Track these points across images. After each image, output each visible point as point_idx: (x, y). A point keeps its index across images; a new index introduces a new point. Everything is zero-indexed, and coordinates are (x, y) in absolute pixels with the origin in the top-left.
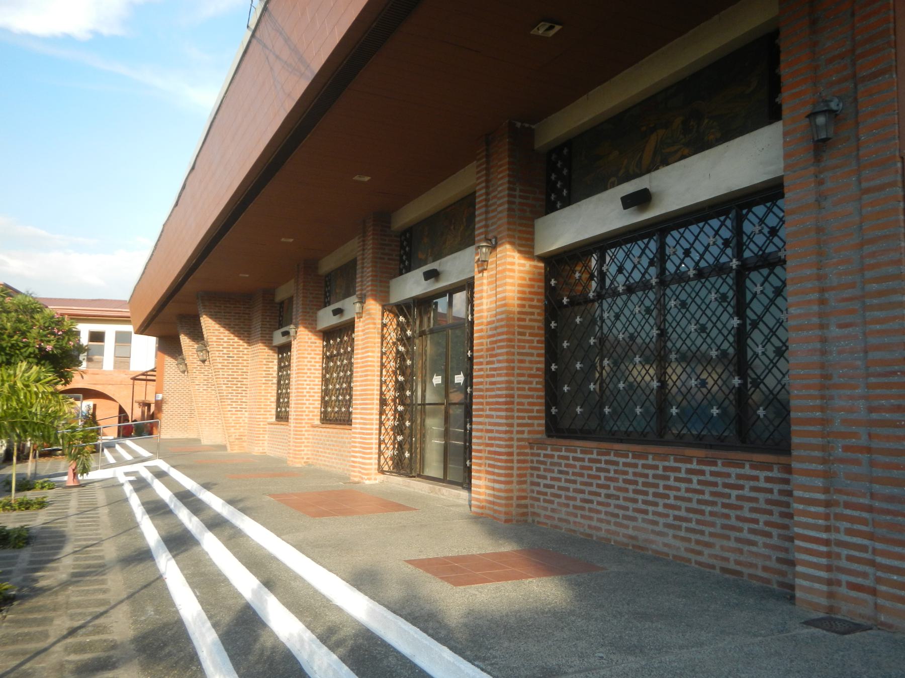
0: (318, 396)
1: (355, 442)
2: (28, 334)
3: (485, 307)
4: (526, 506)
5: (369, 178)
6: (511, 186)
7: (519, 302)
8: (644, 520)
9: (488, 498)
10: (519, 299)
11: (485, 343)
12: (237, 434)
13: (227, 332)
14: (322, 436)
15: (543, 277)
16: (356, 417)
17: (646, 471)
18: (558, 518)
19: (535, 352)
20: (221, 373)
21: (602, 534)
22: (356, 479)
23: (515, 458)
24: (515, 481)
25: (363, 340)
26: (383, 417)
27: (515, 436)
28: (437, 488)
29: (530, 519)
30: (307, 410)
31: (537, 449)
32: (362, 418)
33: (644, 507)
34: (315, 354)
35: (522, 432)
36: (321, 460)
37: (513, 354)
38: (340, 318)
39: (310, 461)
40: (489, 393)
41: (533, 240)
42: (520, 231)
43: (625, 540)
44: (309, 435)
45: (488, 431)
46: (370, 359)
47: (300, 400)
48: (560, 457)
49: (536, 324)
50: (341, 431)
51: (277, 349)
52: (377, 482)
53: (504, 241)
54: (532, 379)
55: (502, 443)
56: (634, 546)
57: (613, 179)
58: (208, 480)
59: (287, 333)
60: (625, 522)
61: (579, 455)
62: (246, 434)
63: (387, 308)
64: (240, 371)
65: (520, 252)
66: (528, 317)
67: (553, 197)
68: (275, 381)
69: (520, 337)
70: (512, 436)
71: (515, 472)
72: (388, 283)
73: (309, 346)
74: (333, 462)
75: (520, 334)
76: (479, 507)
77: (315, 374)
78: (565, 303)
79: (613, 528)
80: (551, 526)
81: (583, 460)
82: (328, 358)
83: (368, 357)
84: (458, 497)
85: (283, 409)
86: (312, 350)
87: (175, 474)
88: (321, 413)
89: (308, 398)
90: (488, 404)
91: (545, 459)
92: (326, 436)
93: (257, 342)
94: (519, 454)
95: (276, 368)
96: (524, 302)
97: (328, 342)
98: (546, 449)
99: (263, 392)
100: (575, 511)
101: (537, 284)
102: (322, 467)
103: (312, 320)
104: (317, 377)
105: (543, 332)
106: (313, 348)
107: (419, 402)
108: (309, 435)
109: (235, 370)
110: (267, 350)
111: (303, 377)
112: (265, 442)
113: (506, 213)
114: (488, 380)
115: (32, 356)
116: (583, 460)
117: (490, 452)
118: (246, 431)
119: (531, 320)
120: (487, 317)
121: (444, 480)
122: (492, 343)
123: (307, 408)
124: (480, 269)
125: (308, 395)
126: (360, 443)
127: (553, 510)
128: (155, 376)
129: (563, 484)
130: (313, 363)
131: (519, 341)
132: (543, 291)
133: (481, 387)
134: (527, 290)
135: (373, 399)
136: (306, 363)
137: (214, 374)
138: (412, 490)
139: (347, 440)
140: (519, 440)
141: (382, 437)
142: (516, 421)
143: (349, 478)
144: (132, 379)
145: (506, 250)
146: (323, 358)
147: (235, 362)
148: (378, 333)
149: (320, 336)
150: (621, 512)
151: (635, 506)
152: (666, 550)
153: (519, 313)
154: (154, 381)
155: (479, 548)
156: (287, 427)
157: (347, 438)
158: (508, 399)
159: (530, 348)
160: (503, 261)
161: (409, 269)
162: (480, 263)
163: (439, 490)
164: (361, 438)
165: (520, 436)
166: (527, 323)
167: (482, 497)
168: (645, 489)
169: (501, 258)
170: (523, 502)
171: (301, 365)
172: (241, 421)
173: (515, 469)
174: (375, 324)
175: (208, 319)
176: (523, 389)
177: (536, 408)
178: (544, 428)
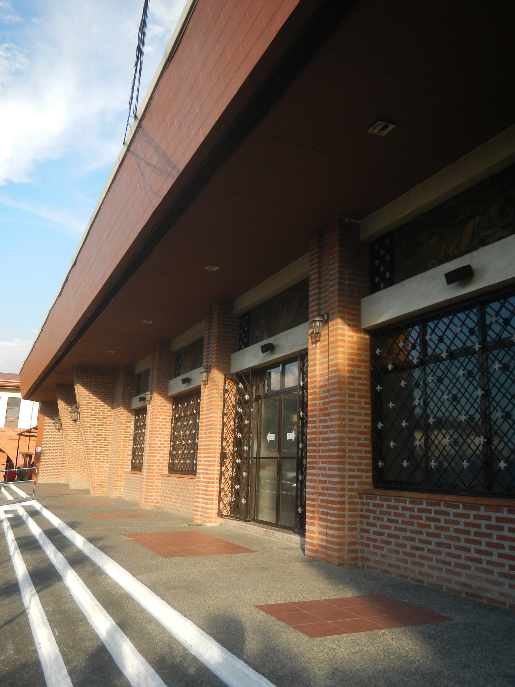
0: (167, 451)
1: (198, 489)
3: (318, 373)
4: (356, 551)
5: (218, 268)
6: (341, 270)
7: (349, 368)
8: (477, 569)
9: (321, 543)
10: (349, 365)
11: (318, 405)
12: (99, 481)
13: (95, 398)
14: (170, 483)
15: (368, 347)
16: (200, 469)
17: (478, 522)
18: (388, 564)
19: (363, 412)
20: (89, 431)
21: (434, 581)
22: (199, 522)
23: (347, 506)
24: (347, 528)
25: (207, 403)
26: (224, 468)
27: (347, 487)
28: (271, 531)
29: (360, 563)
30: (158, 462)
31: (366, 499)
32: (205, 469)
33: (477, 556)
34: (166, 416)
35: (352, 483)
36: (168, 504)
37: (344, 413)
38: (188, 385)
39: (159, 505)
40: (321, 448)
41: (359, 315)
42: (349, 308)
43: (459, 588)
44: (158, 482)
45: (321, 482)
46: (213, 419)
47: (152, 453)
48: (389, 507)
49: (364, 388)
50: (187, 480)
52: (217, 525)
53: (335, 316)
54: (360, 436)
55: (334, 492)
56: (467, 594)
57: (433, 261)
58: (73, 519)
59: (143, 399)
60: (458, 570)
61: (408, 505)
62: (106, 480)
63: (228, 376)
64: (104, 429)
65: (349, 325)
66: (356, 382)
67: (377, 279)
68: (132, 438)
69: (350, 399)
70: (344, 486)
71: (347, 520)
72: (230, 356)
73: (161, 409)
74: (178, 507)
75: (350, 396)
76: (312, 551)
77: (165, 431)
78: (390, 369)
79: (445, 575)
80: (381, 570)
81: (412, 510)
82: (176, 419)
83: (212, 417)
84: (291, 540)
85: (138, 461)
86: (163, 412)
87: (47, 513)
88: (169, 464)
89: (159, 451)
90: (321, 457)
91: (375, 508)
92: (173, 484)
93: (118, 406)
94: (350, 503)
96: (353, 369)
97: (177, 406)
98: (376, 499)
99: (122, 446)
100: (405, 558)
101: (363, 353)
102: (169, 510)
103: (164, 388)
104: (167, 435)
105: (369, 394)
106: (164, 411)
107: (255, 456)
108: (158, 482)
109: (100, 428)
110: (126, 412)
111: (156, 434)
112: (122, 488)
113: (337, 293)
114: (321, 436)
116: (412, 510)
117: (323, 501)
118: (106, 478)
119: (359, 384)
120: (320, 382)
121: (277, 525)
122: (324, 404)
123: (157, 460)
124: (314, 340)
125: (159, 449)
126: (202, 490)
127: (383, 556)
128: (36, 433)
129: (392, 532)
130: (164, 423)
131: (350, 402)
132: (368, 359)
133: (314, 442)
134: (356, 358)
135: (215, 453)
136: (158, 423)
137: (83, 431)
138: (248, 533)
139: (190, 488)
140: (350, 490)
141: (222, 486)
142: (348, 473)
143: (193, 521)
144: (18, 435)
145: (337, 323)
146: (172, 419)
148: (221, 397)
150: (453, 561)
151: (467, 554)
152: (502, 599)
153: (349, 377)
154: (35, 437)
155: (322, 593)
156: (140, 476)
157: (191, 486)
158: (340, 453)
159: (359, 408)
160: (335, 333)
161: (247, 345)
162: (313, 335)
163: (273, 533)
164: (204, 486)
165: (350, 487)
166: (356, 386)
167: (315, 542)
168: (477, 538)
169: (333, 331)
170: (353, 547)
171: (154, 424)
172: (103, 470)
173: (347, 516)
174: (218, 389)
175: (81, 387)
176: (353, 445)
177: (364, 462)
178: (371, 480)
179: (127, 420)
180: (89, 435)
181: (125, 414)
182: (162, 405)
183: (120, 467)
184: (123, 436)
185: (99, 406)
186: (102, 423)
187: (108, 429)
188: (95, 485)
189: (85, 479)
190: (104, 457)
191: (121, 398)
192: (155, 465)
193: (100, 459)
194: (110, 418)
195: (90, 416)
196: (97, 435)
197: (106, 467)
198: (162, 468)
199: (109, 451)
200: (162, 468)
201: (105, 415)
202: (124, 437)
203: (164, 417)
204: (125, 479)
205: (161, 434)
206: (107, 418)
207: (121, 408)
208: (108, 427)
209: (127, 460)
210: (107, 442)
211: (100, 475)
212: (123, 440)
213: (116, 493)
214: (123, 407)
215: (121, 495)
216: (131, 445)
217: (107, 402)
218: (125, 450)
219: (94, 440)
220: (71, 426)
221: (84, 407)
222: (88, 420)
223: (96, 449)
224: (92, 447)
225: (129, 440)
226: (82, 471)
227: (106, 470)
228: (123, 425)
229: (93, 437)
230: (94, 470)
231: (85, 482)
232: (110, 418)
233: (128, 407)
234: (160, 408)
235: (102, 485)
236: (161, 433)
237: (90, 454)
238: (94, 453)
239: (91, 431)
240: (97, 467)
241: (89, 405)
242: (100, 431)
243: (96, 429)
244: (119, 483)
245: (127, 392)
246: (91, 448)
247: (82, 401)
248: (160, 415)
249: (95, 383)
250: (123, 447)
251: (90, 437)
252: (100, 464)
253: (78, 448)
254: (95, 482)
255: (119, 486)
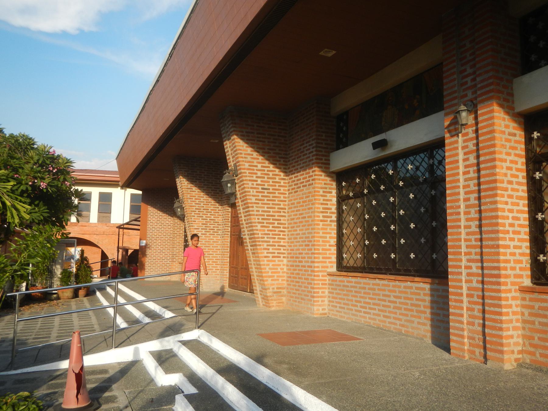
2: (20, 170)
12: (275, 287)
13: (261, 158)
20: (255, 209)
30: (512, 258)
39: (528, 359)
51: (334, 176)
62: (286, 286)
64: (276, 207)
68: (334, 217)
77: (517, 190)
89: (512, 236)
93: (307, 166)
95: (334, 200)
99: (321, 232)
103: (508, 94)
106: (512, 144)
109: (271, 206)
111: (503, 196)
115: (25, 195)
118: (285, 282)
125: (511, 229)
130: (514, 172)
136: (504, 171)
144: (117, 227)
147: (271, 195)
149: (519, 123)
172: (279, 270)
175: (239, 140)
179: (326, 188)
180: (257, 215)
181: (323, 180)
182: (507, 131)
183: (320, 265)
184: (321, 215)
185: (268, 171)
186: (273, 197)
187: (282, 206)
188: (269, 292)
189: (218, 278)
190: (280, 249)
191: (314, 153)
192: (508, 265)
193: (274, 253)
194: (284, 190)
195: (255, 186)
196: (267, 216)
197: (284, 265)
198: (521, 273)
199: (287, 240)
200: (521, 273)
201: (277, 184)
202: (324, 217)
203: (512, 158)
204: (329, 284)
205: (510, 197)
206: (280, 190)
207: (316, 169)
208: (282, 203)
209: (330, 254)
210: (282, 226)
211: (275, 278)
212: (321, 221)
213: (317, 307)
214: (319, 167)
215: (325, 312)
216: (333, 229)
217: (278, 165)
218: (326, 237)
219: (263, 223)
220: (197, 210)
221: (245, 173)
222: (253, 192)
223: (267, 238)
224: (262, 234)
225: (331, 221)
226: (214, 269)
227: (283, 269)
228: (321, 198)
229: (263, 219)
230: (267, 270)
231: (219, 282)
232: (284, 190)
233: (325, 168)
234: (504, 137)
235: (280, 292)
236: (512, 193)
237: (260, 245)
238: (265, 244)
239: (258, 209)
240: (271, 265)
241: (253, 170)
242: (271, 210)
243: (266, 206)
244: (320, 291)
245: (322, 143)
246: (260, 236)
247: (244, 163)
248: (508, 154)
249: (260, 136)
250: (323, 233)
251: (258, 219)
252: (275, 261)
253: (208, 238)
254: (269, 289)
255: (321, 297)
